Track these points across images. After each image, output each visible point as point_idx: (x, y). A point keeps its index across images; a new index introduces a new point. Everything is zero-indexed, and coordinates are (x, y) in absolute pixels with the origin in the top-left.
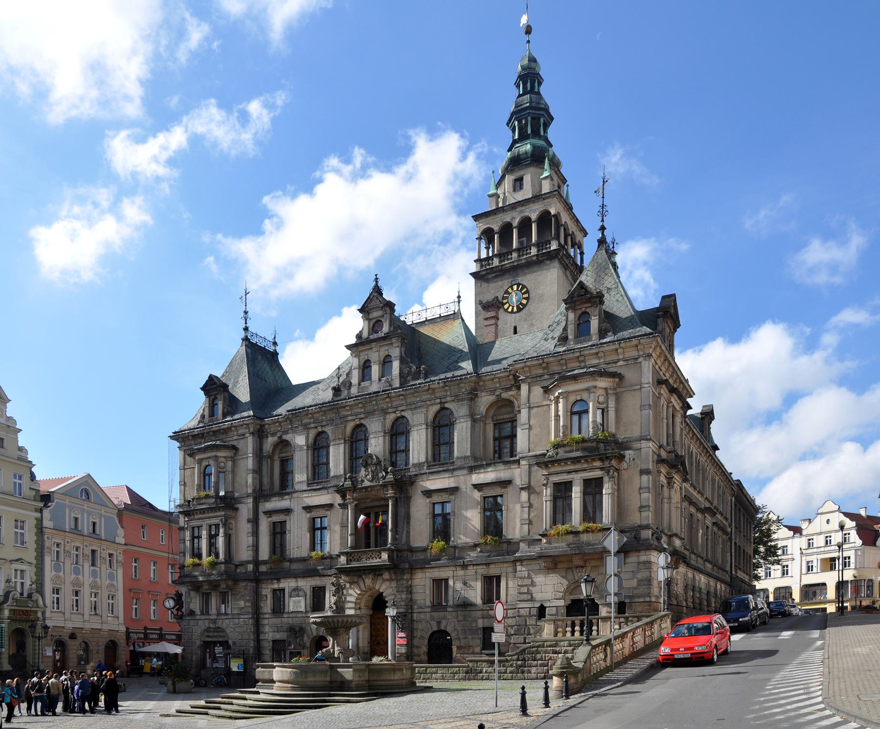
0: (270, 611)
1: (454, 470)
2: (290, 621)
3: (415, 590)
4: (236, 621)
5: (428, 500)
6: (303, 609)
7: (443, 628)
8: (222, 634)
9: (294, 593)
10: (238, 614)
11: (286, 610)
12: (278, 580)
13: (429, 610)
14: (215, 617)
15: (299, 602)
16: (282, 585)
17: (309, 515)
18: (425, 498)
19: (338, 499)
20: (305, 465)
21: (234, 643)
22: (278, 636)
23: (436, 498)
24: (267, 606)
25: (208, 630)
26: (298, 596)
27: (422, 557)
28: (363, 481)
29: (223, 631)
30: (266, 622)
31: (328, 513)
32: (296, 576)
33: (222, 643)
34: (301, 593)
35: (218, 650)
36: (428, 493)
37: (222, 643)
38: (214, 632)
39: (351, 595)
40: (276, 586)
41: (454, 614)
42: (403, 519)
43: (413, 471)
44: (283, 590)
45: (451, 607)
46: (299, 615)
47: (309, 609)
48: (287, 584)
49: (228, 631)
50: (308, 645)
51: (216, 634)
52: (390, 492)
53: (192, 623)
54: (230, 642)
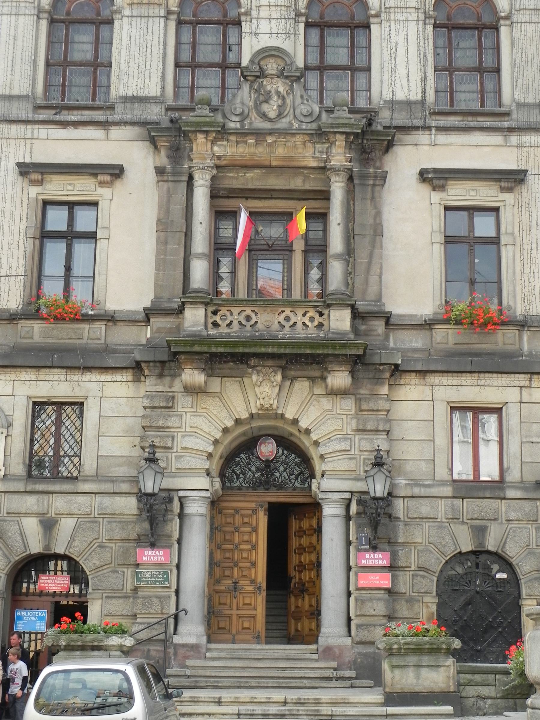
1: (511, 130)
3: (396, 433)
5: (436, 197)
7: (491, 545)
13: (448, 491)
17: (34, 191)
18: (425, 189)
19: (139, 159)
20: (28, 54)
23: (460, 193)
27: (418, 344)
28: (243, 116)
31: (106, 192)
36: (434, 178)
39: (195, 431)
41: (527, 506)
42: (365, 235)
43: (385, 117)
45: (515, 487)
47: (18, 468)
52: (339, 155)
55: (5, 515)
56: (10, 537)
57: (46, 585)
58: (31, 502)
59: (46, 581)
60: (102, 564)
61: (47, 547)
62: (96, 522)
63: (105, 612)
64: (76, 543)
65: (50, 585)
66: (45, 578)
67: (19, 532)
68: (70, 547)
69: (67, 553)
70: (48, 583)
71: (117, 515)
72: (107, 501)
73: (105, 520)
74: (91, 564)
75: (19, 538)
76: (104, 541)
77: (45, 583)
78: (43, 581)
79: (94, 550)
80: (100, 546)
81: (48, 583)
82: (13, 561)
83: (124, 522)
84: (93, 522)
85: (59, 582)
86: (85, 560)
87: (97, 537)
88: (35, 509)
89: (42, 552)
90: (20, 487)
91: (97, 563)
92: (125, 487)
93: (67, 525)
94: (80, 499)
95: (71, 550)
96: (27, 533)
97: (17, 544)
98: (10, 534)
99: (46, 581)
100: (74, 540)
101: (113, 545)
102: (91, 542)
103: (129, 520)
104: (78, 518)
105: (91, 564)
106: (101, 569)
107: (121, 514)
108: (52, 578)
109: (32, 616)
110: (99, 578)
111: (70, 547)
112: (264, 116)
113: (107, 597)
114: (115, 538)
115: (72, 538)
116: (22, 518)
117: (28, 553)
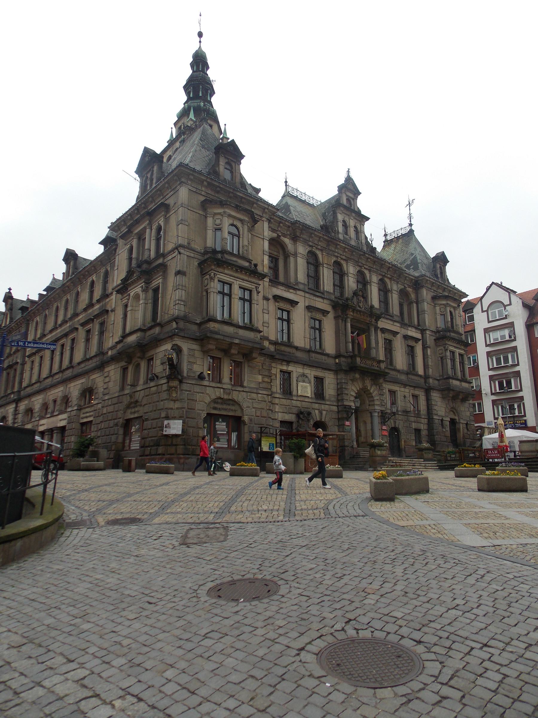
0: (279, 391)
2: (299, 404)
4: (254, 396)
6: (309, 395)
8: (233, 408)
9: (300, 378)
10: (257, 389)
11: (294, 393)
12: (288, 362)
14: (229, 387)
15: (306, 387)
16: (290, 368)
21: (251, 420)
24: (277, 386)
25: (215, 401)
26: (304, 381)
29: (234, 402)
30: (277, 401)
32: (305, 364)
33: (225, 418)
34: (306, 380)
35: (221, 426)
37: (225, 418)
38: (222, 403)
40: (284, 368)
44: (289, 373)
46: (307, 400)
47: (313, 396)
48: (296, 370)
49: (245, 405)
51: (225, 406)
53: (197, 389)
54: (246, 418)
58: (316, 406)
72: (331, 407)
88: (318, 408)
90: (314, 401)
92: (335, 404)
93: (324, 413)
94: (326, 406)
112: (360, 307)
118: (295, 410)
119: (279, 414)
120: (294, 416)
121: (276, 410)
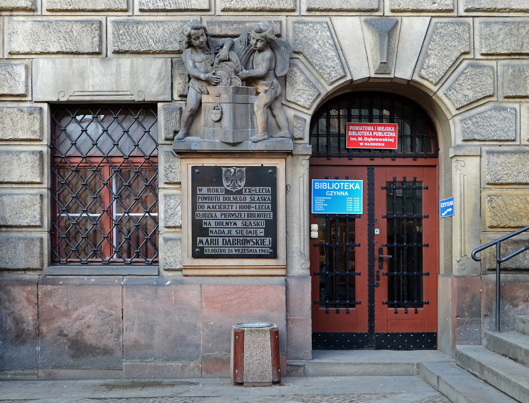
22: (99, 80)
50: (304, 131)
55: (304, 13)
56: (316, 52)
57: (360, 139)
59: (359, 134)
60: (480, 96)
61: (384, 66)
62: (462, 23)
63: (489, 178)
64: (432, 61)
65: (366, 139)
66: (357, 128)
67: (331, 42)
68: (422, 68)
69: (416, 78)
70: (363, 137)
71: (499, 11)
73: (476, 20)
74: (459, 96)
75: (332, 53)
76: (479, 56)
77: (357, 137)
78: (354, 133)
79: (462, 73)
80: (472, 66)
81: (363, 137)
82: (324, 93)
83: (514, 23)
84: (458, 24)
85: (380, 134)
86: (449, 89)
87: (467, 49)
89: (373, 75)
91: (471, 95)
95: (423, 73)
96: (345, 43)
97: (330, 64)
98: (316, 46)
99: (359, 134)
100: (427, 55)
101: (493, 63)
102: (457, 59)
103: (518, 19)
104: (432, 17)
105: (459, 96)
106: (475, 105)
107: (504, 10)
108: (369, 128)
109: (340, 190)
110: (474, 120)
111: (422, 68)
113: (488, 152)
114: (499, 51)
115: (423, 53)
116: (334, 18)
117: (349, 78)
118: (169, 31)
119: (43, 65)
120: (157, 66)
121: (20, 44)
